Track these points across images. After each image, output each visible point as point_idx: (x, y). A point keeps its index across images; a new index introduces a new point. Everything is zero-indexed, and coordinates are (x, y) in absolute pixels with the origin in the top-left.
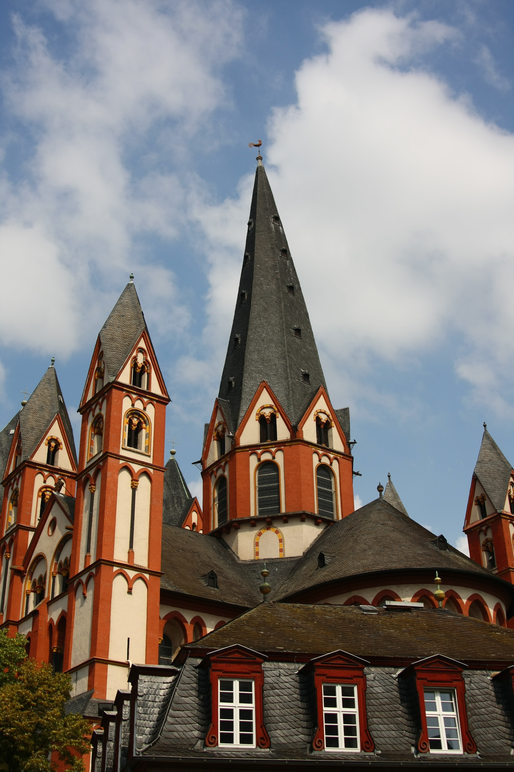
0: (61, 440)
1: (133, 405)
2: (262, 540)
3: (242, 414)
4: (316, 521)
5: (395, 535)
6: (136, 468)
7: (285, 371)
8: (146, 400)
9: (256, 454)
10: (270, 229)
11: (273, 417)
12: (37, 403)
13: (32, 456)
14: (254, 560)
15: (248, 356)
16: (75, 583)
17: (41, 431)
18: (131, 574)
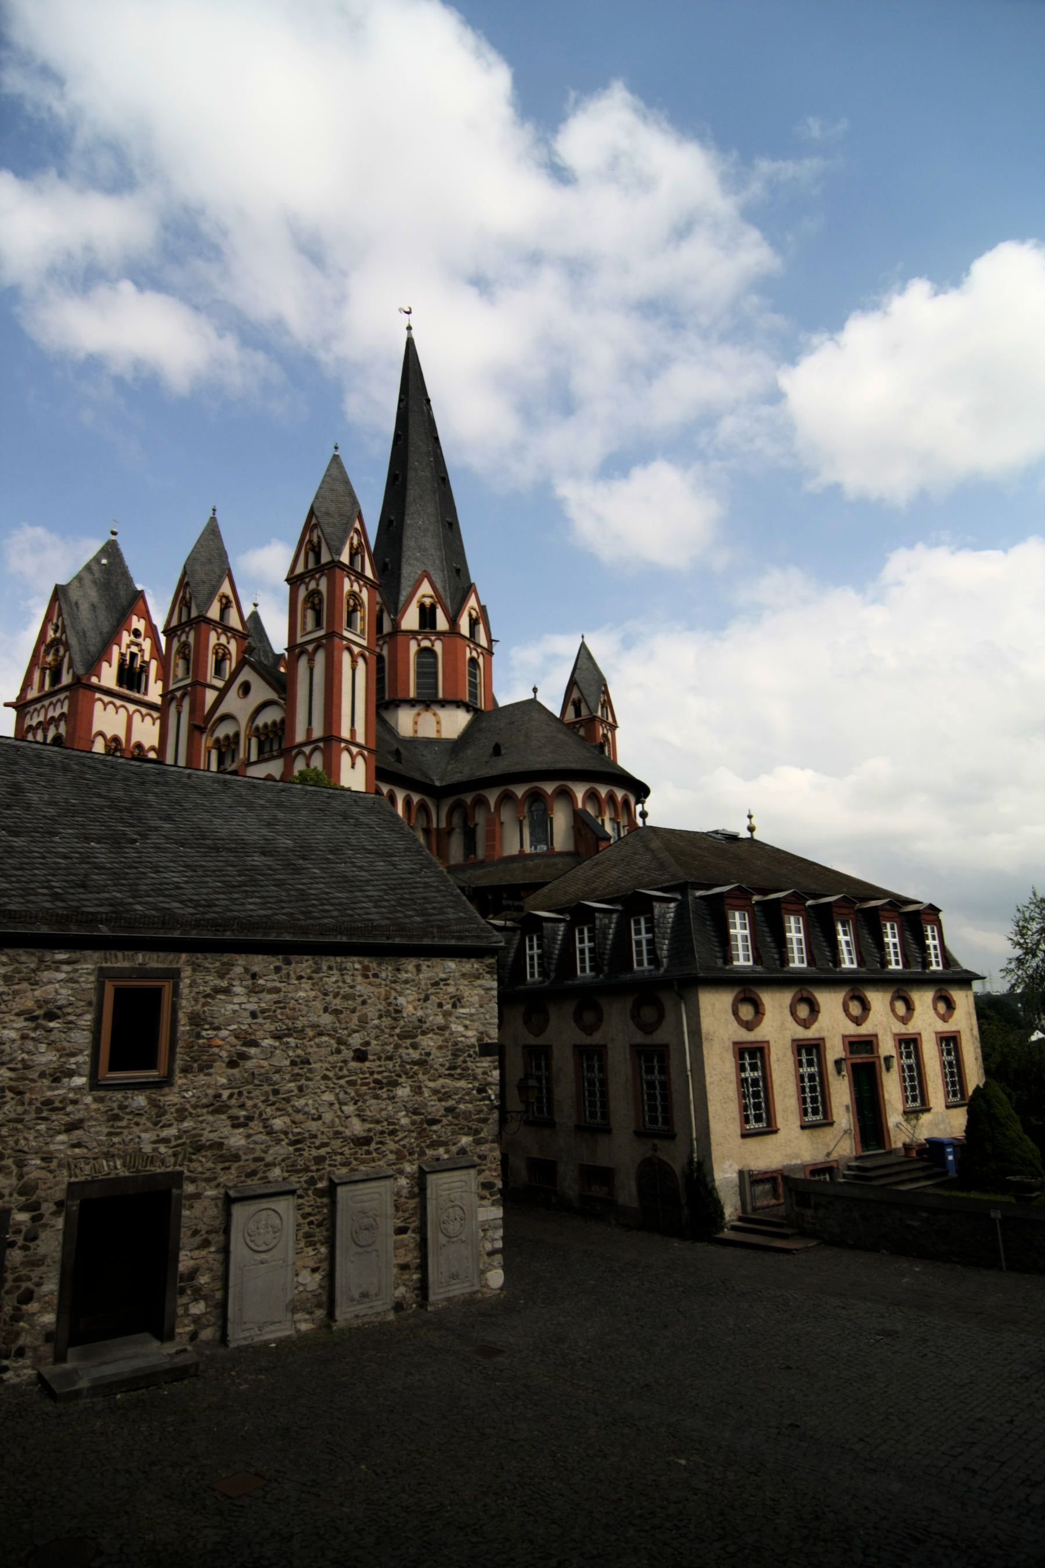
1: (352, 586)
2: (420, 720)
3: (402, 598)
4: (468, 708)
5: (561, 736)
6: (356, 650)
7: (442, 563)
8: (361, 583)
9: (417, 639)
10: (423, 411)
12: (203, 554)
13: (207, 612)
15: (405, 542)
16: (294, 752)
17: (213, 586)
18: (355, 750)
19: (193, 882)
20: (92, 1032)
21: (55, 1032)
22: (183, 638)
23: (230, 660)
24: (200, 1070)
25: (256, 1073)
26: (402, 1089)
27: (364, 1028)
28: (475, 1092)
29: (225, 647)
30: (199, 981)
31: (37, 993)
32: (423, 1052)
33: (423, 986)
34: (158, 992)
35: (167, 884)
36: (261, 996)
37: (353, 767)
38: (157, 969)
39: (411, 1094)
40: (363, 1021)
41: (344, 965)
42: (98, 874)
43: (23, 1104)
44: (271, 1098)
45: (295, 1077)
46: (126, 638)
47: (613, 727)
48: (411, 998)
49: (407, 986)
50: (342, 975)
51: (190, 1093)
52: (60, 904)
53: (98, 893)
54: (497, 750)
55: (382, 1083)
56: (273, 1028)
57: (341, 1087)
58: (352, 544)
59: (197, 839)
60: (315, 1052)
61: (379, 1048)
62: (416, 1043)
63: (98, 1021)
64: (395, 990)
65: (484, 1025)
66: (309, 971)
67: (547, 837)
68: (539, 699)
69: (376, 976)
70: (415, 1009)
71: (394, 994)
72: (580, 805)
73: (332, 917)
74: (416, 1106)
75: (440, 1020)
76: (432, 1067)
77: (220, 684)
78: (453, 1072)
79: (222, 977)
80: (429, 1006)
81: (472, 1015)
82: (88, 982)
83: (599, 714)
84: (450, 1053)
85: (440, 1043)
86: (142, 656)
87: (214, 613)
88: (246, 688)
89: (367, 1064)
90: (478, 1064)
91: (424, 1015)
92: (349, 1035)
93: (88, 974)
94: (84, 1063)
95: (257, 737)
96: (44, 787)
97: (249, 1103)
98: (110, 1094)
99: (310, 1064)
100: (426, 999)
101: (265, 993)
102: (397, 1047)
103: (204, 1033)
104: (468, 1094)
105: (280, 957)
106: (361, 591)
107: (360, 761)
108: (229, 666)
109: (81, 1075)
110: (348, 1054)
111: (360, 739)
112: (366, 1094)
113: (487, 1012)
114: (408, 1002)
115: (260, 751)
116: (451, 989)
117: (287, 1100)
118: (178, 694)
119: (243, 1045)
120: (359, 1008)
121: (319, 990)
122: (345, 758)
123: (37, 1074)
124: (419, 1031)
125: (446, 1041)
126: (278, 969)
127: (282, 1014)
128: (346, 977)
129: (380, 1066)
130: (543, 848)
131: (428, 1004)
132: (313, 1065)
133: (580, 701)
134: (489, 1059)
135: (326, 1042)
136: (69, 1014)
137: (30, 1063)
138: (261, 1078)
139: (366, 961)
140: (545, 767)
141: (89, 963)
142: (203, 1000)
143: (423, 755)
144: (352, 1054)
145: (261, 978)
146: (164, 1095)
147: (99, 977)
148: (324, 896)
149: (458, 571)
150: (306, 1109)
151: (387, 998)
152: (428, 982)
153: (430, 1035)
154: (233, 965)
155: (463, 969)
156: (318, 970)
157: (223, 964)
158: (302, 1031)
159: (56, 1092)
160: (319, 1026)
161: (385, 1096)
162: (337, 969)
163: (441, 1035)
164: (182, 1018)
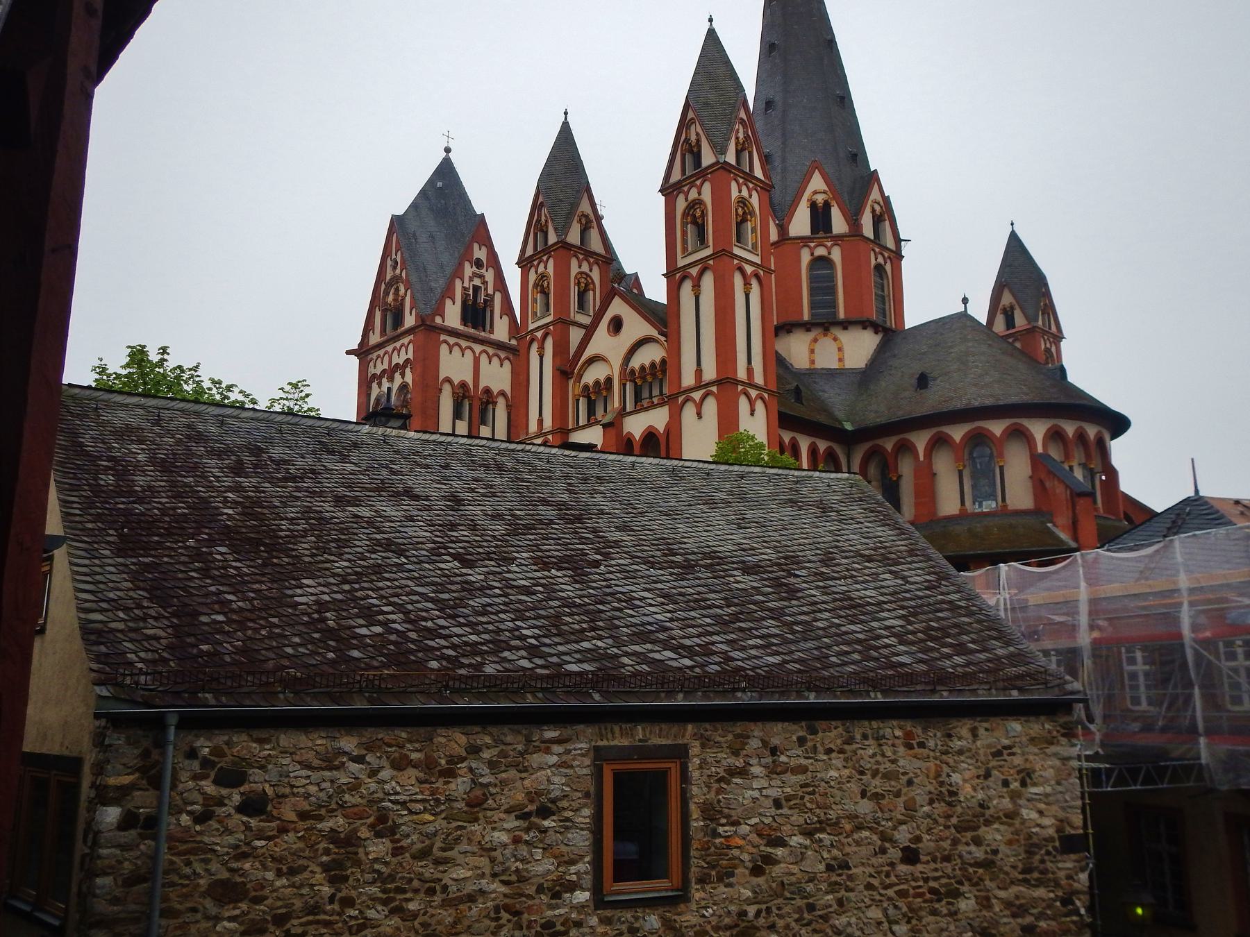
0: (592, 216)
1: (740, 191)
2: (817, 347)
4: (876, 327)
6: (749, 269)
8: (751, 185)
9: (808, 246)
11: (827, 205)
14: (810, 369)
16: (680, 399)
17: (571, 204)
18: (753, 393)
19: (678, 620)
20: (592, 832)
21: (551, 832)
22: (541, 269)
23: (594, 290)
24: (720, 879)
25: (786, 882)
26: (966, 901)
27: (912, 817)
28: (1058, 904)
29: (588, 275)
30: (709, 760)
31: (526, 782)
32: (988, 849)
33: (982, 758)
34: (664, 773)
35: (650, 624)
36: (785, 777)
37: (752, 413)
38: (661, 746)
39: (977, 908)
40: (911, 807)
41: (881, 732)
42: (570, 615)
43: (521, 928)
44: (806, 915)
45: (833, 887)
46: (468, 270)
47: (1058, 337)
48: (967, 775)
49: (962, 758)
50: (880, 745)
51: (710, 910)
52: (540, 662)
53: (577, 642)
54: (923, 381)
55: (941, 893)
56: (801, 821)
57: (890, 899)
58: (737, 138)
59: (666, 555)
60: (855, 853)
61: (932, 844)
62: (978, 837)
63: (598, 817)
64: (947, 764)
65: (1063, 809)
66: (839, 742)
67: (995, 491)
68: (969, 312)
69: (922, 745)
70: (975, 790)
71: (946, 769)
72: (1040, 449)
73: (854, 662)
74: (985, 924)
75: (1006, 803)
76: (1001, 870)
77: (586, 320)
78: (1028, 876)
79: (736, 753)
80: (991, 784)
81: (1047, 795)
82: (583, 767)
83: (1040, 323)
84: (1021, 850)
85: (1009, 836)
86: (486, 289)
87: (574, 237)
88: (617, 325)
89: (920, 867)
90: (1060, 865)
91: (986, 798)
92: (895, 828)
93: (582, 755)
94: (586, 873)
95: (633, 381)
96: (483, 495)
97: (780, 923)
98: (618, 913)
99: (849, 868)
100: (987, 775)
101: (789, 773)
102: (955, 842)
103: (720, 829)
104: (1049, 907)
105: (803, 724)
106: (750, 196)
107: (759, 406)
108: (594, 298)
109: (583, 889)
110: (894, 854)
111: (759, 379)
112: (921, 908)
113: (1067, 791)
114: (965, 781)
115: (638, 398)
116: (1017, 760)
117: (825, 918)
118: (539, 334)
119: (768, 844)
120: (904, 790)
121: (854, 768)
122: (743, 404)
123: (534, 888)
124: (981, 819)
125: (1017, 833)
126: (802, 741)
127: (811, 801)
128: (884, 748)
129: (936, 870)
130: (989, 506)
131: (990, 782)
132: (854, 871)
133: (1012, 308)
134: (1073, 857)
135: (866, 838)
136: (564, 809)
137: (525, 874)
138: (792, 888)
139: (908, 725)
140: (989, 402)
141: (583, 742)
142: (717, 785)
143: (824, 391)
144: (900, 854)
145: (782, 754)
146: (679, 914)
147: (595, 759)
148: (834, 630)
149: (856, 155)
150: (849, 930)
151: (938, 775)
152: (989, 751)
153: (995, 826)
154: (748, 737)
155: (1031, 731)
156: (850, 740)
157: (737, 736)
158: (837, 823)
159: (557, 912)
160: (857, 817)
161: (945, 911)
162: (873, 738)
163: (1010, 825)
164: (695, 812)
